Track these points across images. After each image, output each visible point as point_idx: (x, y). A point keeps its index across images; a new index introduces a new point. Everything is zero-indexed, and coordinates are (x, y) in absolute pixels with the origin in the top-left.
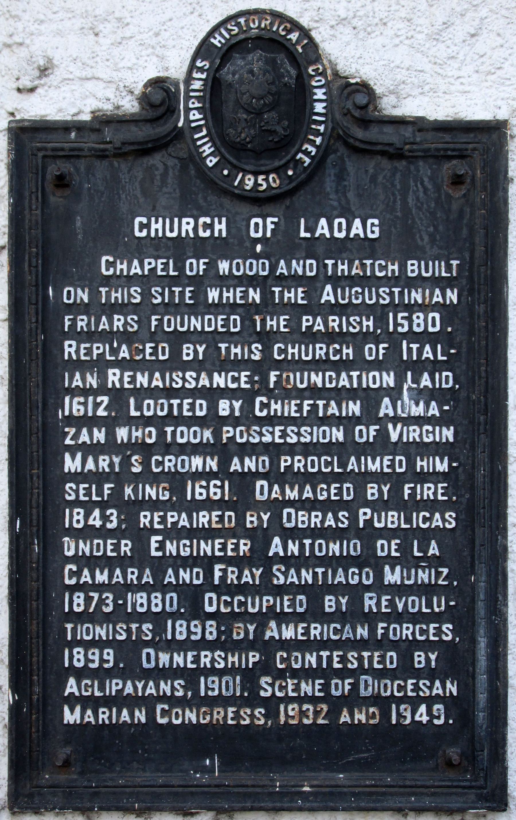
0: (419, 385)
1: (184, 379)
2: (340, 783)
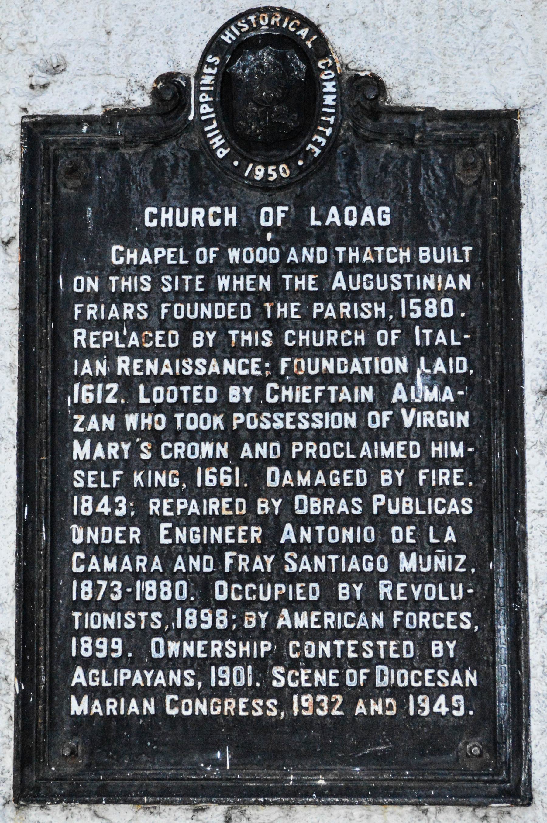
0: (432, 370)
1: (194, 366)
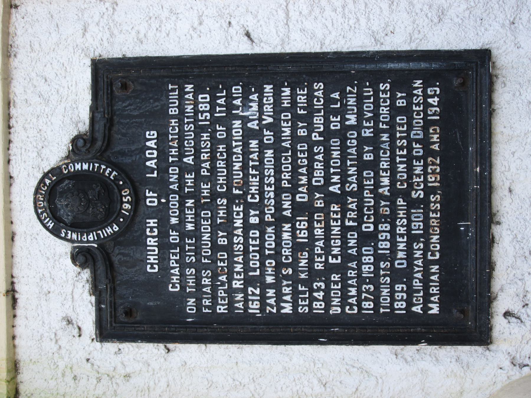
0: (240, 106)
1: (238, 244)
2: (475, 150)
